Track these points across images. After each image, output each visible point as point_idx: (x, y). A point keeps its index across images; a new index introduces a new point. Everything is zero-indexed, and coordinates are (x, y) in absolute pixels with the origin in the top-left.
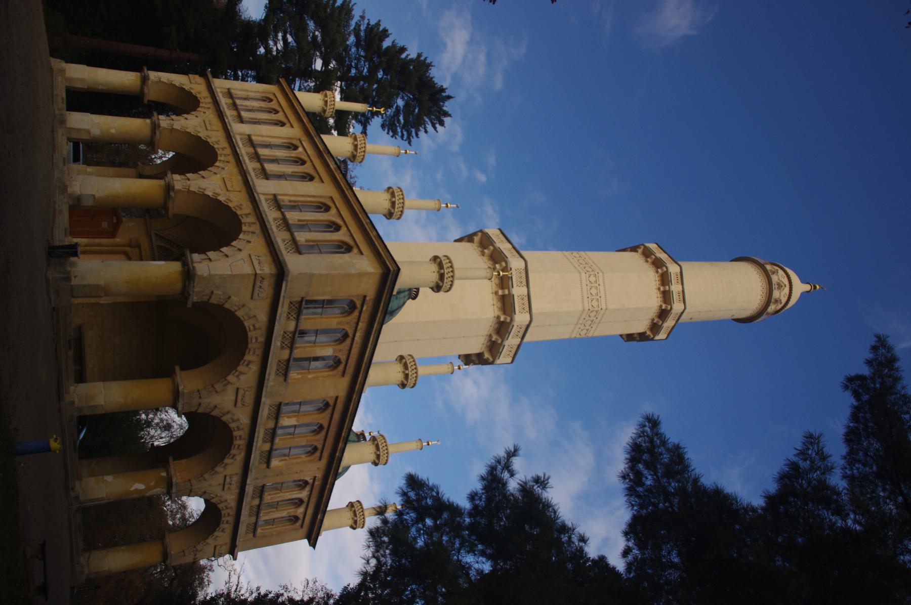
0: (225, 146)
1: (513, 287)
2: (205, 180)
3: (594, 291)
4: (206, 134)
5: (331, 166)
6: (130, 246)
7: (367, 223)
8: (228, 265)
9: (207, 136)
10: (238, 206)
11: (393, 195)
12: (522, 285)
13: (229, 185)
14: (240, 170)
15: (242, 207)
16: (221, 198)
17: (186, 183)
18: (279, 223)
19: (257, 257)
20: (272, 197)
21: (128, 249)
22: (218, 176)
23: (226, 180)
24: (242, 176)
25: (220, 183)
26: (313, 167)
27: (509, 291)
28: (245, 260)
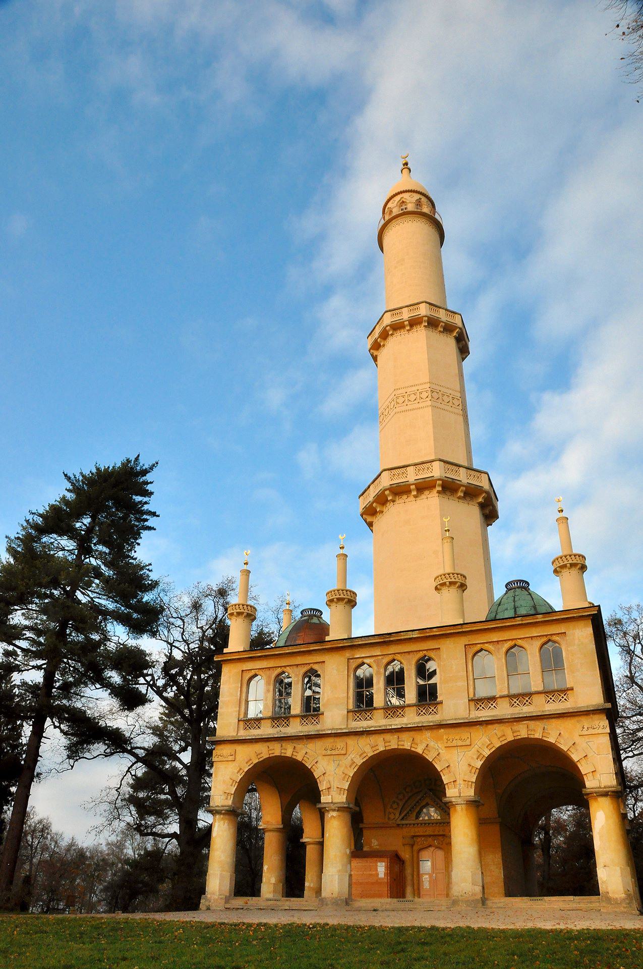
0: (382, 739)
1: (461, 481)
2: (452, 765)
3: (446, 399)
4: (358, 757)
5: (414, 636)
6: (412, 846)
7: (522, 620)
8: (598, 756)
9: (360, 756)
10: (499, 739)
11: (443, 584)
12: (431, 467)
13: (460, 743)
14: (426, 730)
15: (499, 734)
16: (487, 753)
17: (460, 784)
18: (518, 702)
19: (584, 729)
20: (472, 704)
21: (416, 848)
22: (440, 751)
23: (450, 744)
24: (441, 728)
25: (454, 751)
26: (406, 654)
27: (463, 486)
28: (588, 740)
